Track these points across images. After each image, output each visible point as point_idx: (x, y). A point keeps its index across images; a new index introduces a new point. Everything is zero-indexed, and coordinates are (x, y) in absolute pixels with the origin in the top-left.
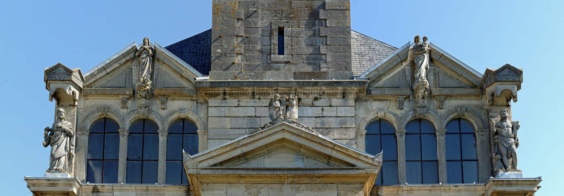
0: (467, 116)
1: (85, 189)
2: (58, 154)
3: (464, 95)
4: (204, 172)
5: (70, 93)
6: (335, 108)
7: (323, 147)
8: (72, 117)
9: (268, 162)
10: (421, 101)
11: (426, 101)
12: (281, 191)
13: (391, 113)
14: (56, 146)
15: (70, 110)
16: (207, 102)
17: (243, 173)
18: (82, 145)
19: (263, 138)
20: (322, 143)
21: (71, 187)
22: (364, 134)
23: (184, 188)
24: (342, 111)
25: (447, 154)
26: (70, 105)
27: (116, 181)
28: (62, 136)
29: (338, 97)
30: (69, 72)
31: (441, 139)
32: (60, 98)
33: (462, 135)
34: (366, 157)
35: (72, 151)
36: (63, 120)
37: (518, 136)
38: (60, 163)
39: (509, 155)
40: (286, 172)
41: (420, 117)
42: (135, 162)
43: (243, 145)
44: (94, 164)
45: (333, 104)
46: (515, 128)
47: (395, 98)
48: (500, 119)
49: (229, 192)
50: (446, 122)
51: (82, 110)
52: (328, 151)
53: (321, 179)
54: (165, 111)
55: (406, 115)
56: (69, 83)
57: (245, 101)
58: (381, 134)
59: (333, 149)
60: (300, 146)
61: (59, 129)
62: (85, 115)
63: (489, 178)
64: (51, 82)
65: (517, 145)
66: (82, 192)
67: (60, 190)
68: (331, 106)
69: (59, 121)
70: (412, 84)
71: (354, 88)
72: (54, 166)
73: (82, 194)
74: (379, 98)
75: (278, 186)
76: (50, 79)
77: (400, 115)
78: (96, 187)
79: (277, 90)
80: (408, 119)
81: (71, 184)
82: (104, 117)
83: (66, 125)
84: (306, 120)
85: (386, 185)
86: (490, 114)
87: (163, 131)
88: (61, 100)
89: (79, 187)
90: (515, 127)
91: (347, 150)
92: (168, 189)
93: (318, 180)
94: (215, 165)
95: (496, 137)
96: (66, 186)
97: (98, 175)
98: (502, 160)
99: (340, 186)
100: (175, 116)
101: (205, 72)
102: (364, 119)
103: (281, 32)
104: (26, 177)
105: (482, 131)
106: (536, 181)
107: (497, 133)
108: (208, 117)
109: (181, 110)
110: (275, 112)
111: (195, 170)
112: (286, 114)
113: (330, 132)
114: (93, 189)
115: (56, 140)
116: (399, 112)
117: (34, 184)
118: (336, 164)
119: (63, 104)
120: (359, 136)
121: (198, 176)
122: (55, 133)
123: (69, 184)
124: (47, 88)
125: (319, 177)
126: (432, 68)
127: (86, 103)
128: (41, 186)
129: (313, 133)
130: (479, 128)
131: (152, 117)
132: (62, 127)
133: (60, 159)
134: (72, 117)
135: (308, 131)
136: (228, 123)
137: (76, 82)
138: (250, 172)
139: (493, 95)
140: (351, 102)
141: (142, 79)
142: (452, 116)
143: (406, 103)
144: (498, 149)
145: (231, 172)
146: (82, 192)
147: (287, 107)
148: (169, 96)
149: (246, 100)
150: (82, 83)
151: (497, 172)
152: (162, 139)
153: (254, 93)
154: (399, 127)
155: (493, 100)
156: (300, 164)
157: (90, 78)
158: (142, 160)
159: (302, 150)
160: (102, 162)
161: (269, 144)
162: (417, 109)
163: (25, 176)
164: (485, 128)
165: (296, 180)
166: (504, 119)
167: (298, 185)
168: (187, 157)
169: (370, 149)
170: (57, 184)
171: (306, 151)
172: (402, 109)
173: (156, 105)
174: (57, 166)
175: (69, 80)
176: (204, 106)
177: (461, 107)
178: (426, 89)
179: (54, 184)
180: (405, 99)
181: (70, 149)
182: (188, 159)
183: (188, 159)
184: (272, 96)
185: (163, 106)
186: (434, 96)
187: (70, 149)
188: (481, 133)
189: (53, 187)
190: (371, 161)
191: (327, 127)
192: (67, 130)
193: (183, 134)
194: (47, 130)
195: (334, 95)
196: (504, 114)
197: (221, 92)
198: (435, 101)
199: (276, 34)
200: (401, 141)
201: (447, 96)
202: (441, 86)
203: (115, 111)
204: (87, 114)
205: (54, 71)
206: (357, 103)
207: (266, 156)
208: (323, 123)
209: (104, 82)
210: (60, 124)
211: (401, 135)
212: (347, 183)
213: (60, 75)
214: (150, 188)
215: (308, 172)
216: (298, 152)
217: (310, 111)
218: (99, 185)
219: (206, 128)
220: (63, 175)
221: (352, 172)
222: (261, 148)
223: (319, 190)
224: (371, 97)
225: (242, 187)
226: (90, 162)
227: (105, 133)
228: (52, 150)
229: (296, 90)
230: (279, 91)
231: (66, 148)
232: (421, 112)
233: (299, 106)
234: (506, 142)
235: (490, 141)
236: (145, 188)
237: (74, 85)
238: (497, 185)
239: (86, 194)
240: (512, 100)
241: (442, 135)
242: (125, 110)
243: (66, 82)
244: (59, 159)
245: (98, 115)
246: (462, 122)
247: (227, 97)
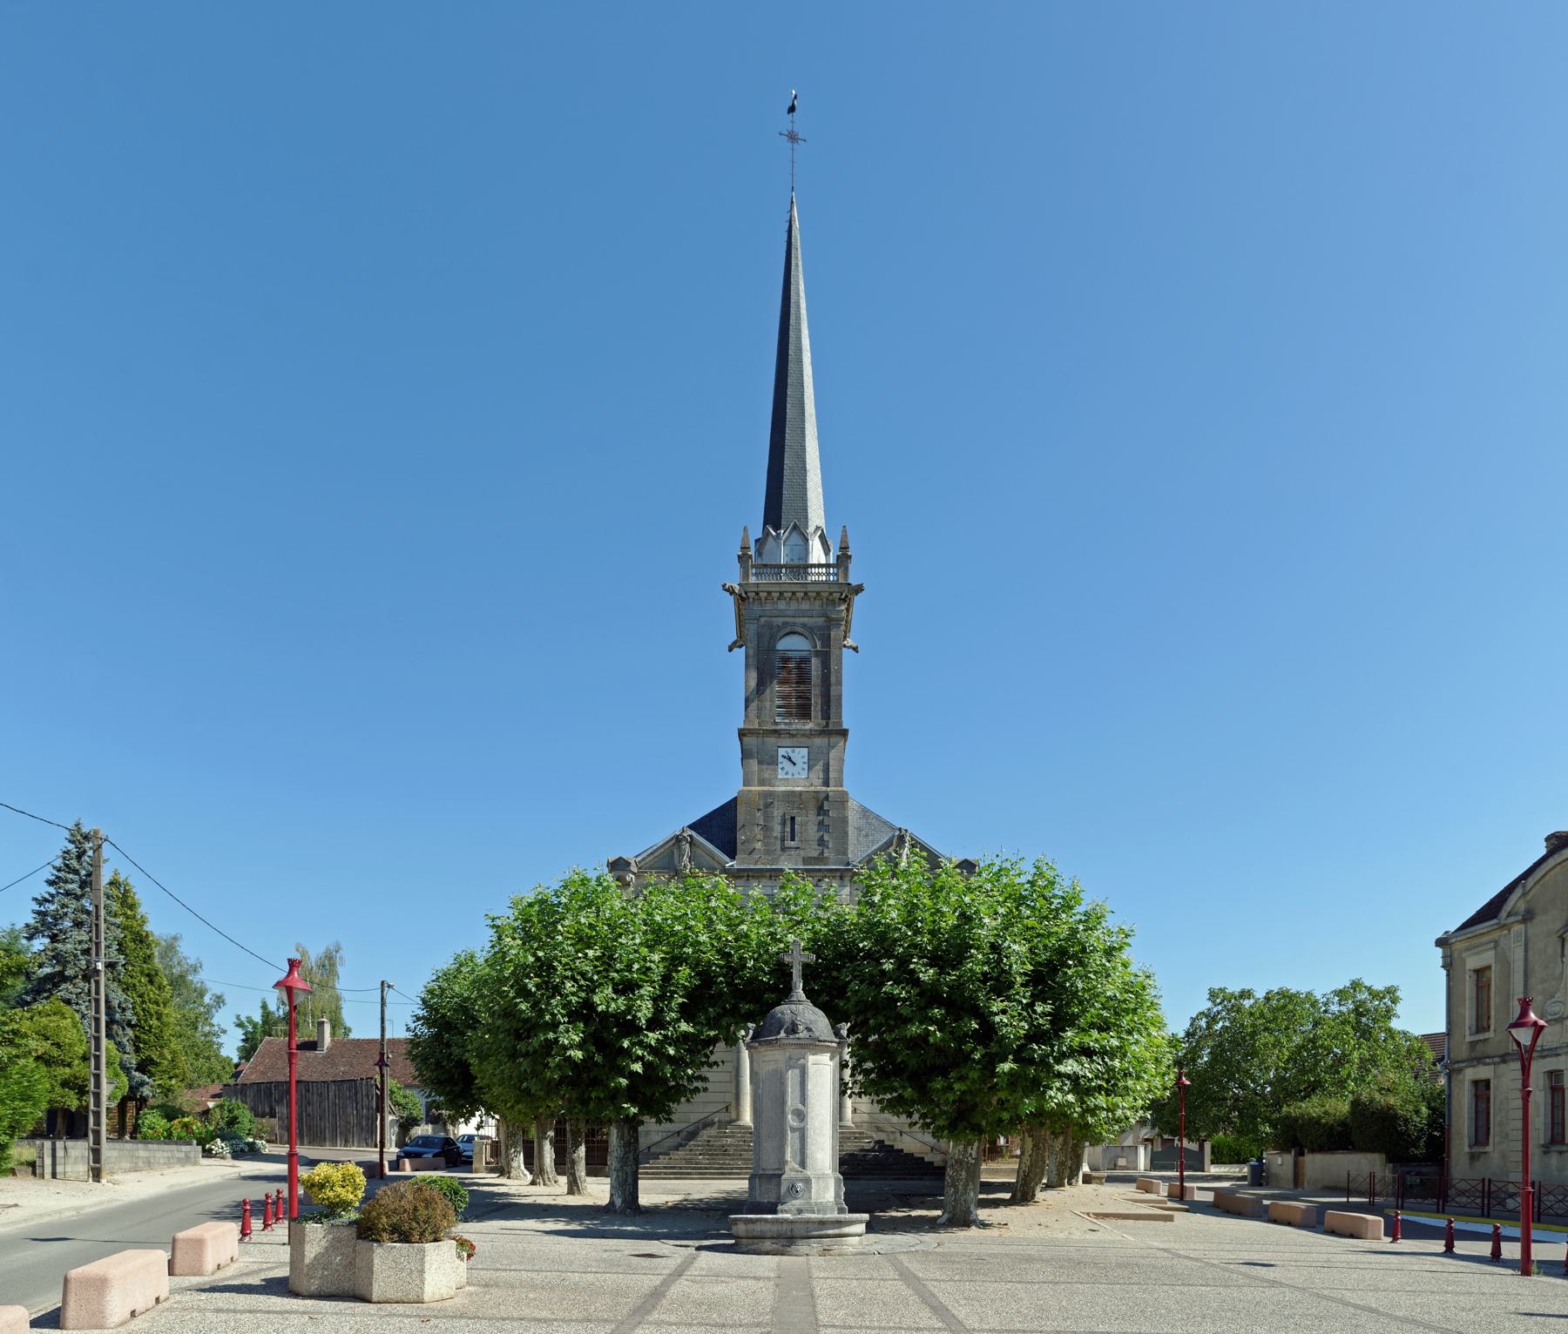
101: (732, 856)
103: (793, 819)
199: (788, 823)
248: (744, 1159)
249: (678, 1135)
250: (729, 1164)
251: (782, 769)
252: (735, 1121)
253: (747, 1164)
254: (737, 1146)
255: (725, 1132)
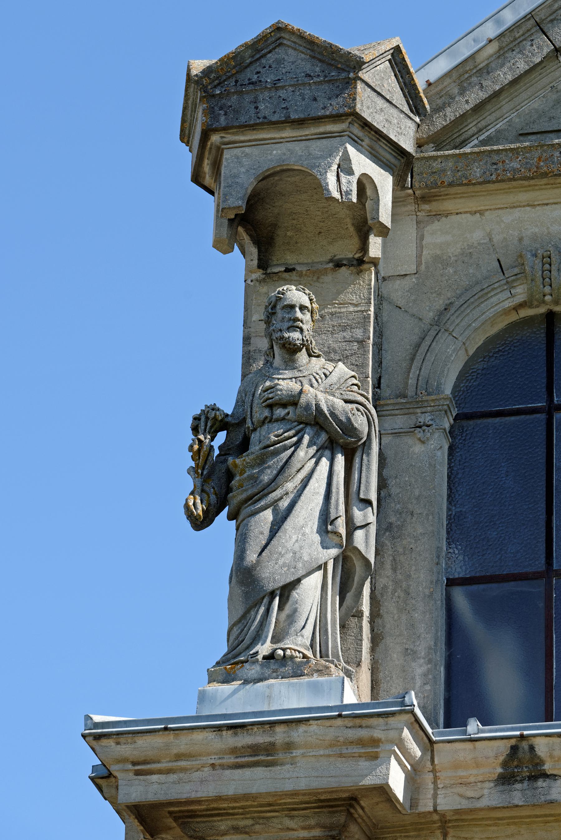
1: (456, 766)
2: (281, 562)
5: (348, 193)
8: (347, 335)
14: (268, 515)
15: (339, 293)
18: (417, 493)
21: (375, 757)
26: (338, 265)
32: (275, 226)
35: (359, 535)
36: (302, 356)
38: (292, 618)
51: (408, 283)
56: (340, 134)
61: (280, 412)
64: (229, 137)
66: (436, 788)
67: (303, 785)
69: (277, 361)
72: (258, 638)
73: (435, 796)
76: (222, 118)
78: (525, 745)
81: (375, 742)
82: (542, 310)
88: (279, 241)
89: (418, 753)
96: (341, 755)
104: (97, 718)
114: (505, 764)
115: (266, 478)
117: (145, 762)
119: (291, 259)
122: (254, 437)
123: (361, 742)
124: (197, 178)
127: (428, 239)
128: (183, 770)
132: (303, 400)
133: (295, 594)
134: (347, 335)
137: (378, 122)
146: (435, 783)
150: (409, 123)
157: (456, 91)
163: (88, 718)
170: (289, 746)
174: (276, 639)
175: (336, 118)
181: (351, 527)
189: (259, 771)
192: (332, 414)
204: (440, 304)
205: (250, 74)
209: (536, 104)
213: (282, 93)
220: (315, 688)
237: (367, 141)
239: (461, 796)
243: (322, 129)
245: (508, 304)
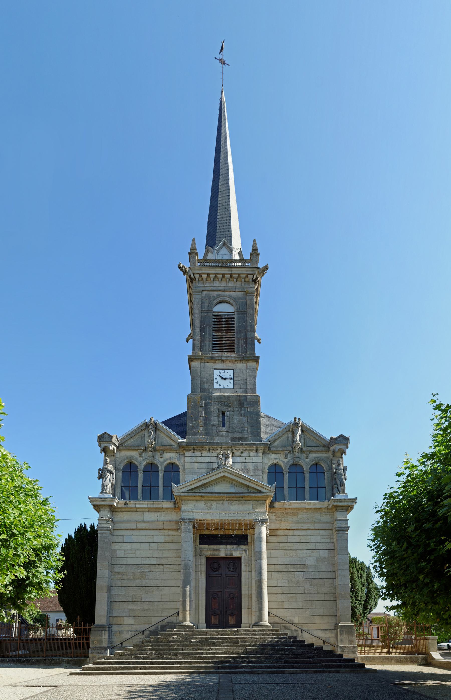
0: (321, 463)
3: (319, 451)
4: (183, 494)
6: (252, 458)
7: (245, 481)
9: (217, 489)
10: (297, 454)
11: (299, 454)
12: (223, 505)
13: (281, 461)
16: (185, 454)
17: (203, 495)
19: (214, 475)
20: (244, 478)
22: (267, 472)
23: (173, 503)
24: (256, 460)
25: (310, 484)
27: (137, 499)
28: (108, 473)
29: (254, 451)
30: (111, 437)
31: (307, 475)
33: (318, 473)
34: (267, 486)
37: (347, 474)
39: (341, 485)
40: (225, 495)
41: (296, 463)
42: (147, 488)
43: (203, 480)
44: (125, 488)
45: (251, 455)
46: (345, 470)
47: (283, 452)
48: (337, 465)
49: (196, 505)
50: (309, 466)
52: (247, 483)
53: (244, 498)
54: (162, 459)
55: (289, 462)
57: (205, 453)
58: (276, 473)
59: (250, 482)
60: (233, 480)
62: (120, 461)
63: (330, 498)
65: (346, 479)
68: (249, 456)
70: (292, 444)
71: (262, 447)
72: (104, 490)
74: (275, 452)
75: (221, 502)
77: (286, 462)
79: (221, 447)
80: (290, 464)
83: (110, 467)
84: (236, 464)
85: (278, 501)
86: (333, 462)
87: (161, 470)
90: (345, 469)
91: (257, 482)
92: (165, 503)
93: (242, 499)
94: (189, 490)
95: (335, 475)
97: (127, 495)
98: (337, 488)
99: (254, 502)
100: (168, 462)
101: (183, 437)
102: (267, 464)
103: (224, 414)
105: (328, 471)
106: (354, 500)
107: (335, 473)
108: (185, 462)
109: (171, 458)
110: (220, 461)
111: (178, 493)
112: (225, 462)
113: (249, 471)
116: (286, 460)
118: (251, 490)
120: (264, 474)
121: (179, 496)
125: (243, 497)
126: (303, 435)
129: (240, 473)
130: (326, 470)
131: (156, 462)
135: (237, 472)
136: (196, 466)
138: (207, 495)
139: (334, 451)
140: (260, 454)
141: (150, 441)
142: (313, 463)
143: (289, 455)
144: (336, 482)
145: (197, 494)
147: (226, 458)
148: (164, 450)
149: (206, 453)
151: (335, 494)
152: (161, 475)
153: (209, 449)
154: (286, 469)
155: (334, 454)
156: (233, 490)
158: (151, 487)
159: (234, 482)
160: (129, 488)
161: (217, 479)
162: (295, 458)
164: (330, 469)
165: (231, 498)
166: (339, 465)
167: (232, 502)
168: (174, 486)
169: (270, 483)
171: (236, 483)
172: (287, 458)
173: (158, 455)
176: (183, 456)
177: (317, 458)
178: (299, 447)
179: (104, 501)
180: (288, 453)
181: (112, 481)
182: (175, 487)
183: (175, 487)
184: (219, 451)
185: (161, 456)
186: (304, 451)
187: (112, 481)
188: (328, 473)
190: (269, 489)
191: (248, 468)
193: (172, 472)
194: (100, 470)
195: (251, 450)
196: (339, 462)
197: (192, 448)
198: (304, 454)
199: (221, 415)
200: (286, 476)
201: (310, 452)
202: (307, 446)
203: (136, 459)
206: (264, 455)
207: (215, 485)
208: (245, 466)
209: (130, 442)
210: (106, 467)
211: (286, 473)
212: (257, 501)
214: (155, 502)
215: (237, 495)
216: (232, 483)
217: (239, 459)
218: (128, 501)
219: (184, 469)
220: (109, 495)
221: (260, 495)
222: (212, 481)
223: (243, 504)
224: (271, 451)
225: (203, 502)
226: (123, 488)
227: (130, 471)
228: (103, 481)
229: (231, 447)
230: (223, 448)
231: (110, 480)
232: (297, 460)
233: (233, 456)
234: (340, 478)
235: (332, 477)
236: (152, 503)
238: (334, 502)
240: (344, 454)
241: (307, 473)
242: (141, 458)
244: (107, 486)
246: (318, 466)
247: (195, 451)
248: (184, 654)
249: (143, 634)
250: (172, 659)
251: (217, 383)
252: (182, 622)
253: (187, 658)
254: (180, 642)
255: (174, 631)
